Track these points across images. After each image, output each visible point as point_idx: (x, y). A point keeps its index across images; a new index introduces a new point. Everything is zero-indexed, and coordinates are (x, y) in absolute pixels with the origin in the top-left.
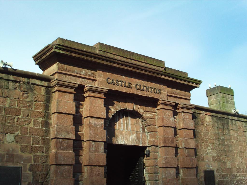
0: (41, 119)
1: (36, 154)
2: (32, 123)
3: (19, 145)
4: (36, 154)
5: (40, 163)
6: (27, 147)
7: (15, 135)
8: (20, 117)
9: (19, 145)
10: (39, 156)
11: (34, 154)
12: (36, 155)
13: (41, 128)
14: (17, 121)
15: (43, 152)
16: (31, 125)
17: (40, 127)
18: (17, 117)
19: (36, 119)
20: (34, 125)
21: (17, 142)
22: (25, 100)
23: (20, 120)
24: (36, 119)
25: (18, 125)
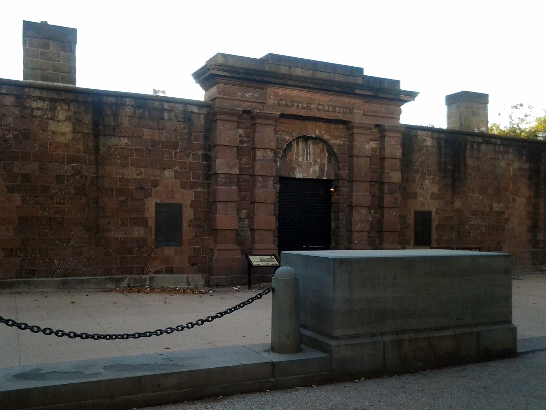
0: (200, 152)
1: (196, 190)
2: (191, 156)
3: (178, 181)
4: (196, 190)
5: (201, 199)
6: (187, 182)
7: (174, 170)
8: (178, 150)
9: (178, 181)
10: (200, 192)
11: (194, 190)
12: (197, 191)
13: (201, 162)
14: (175, 156)
15: (204, 188)
16: (190, 159)
17: (200, 161)
18: (174, 151)
19: (195, 152)
20: (194, 159)
21: (176, 178)
22: (183, 131)
23: (178, 154)
24: (195, 152)
25: (176, 160)
